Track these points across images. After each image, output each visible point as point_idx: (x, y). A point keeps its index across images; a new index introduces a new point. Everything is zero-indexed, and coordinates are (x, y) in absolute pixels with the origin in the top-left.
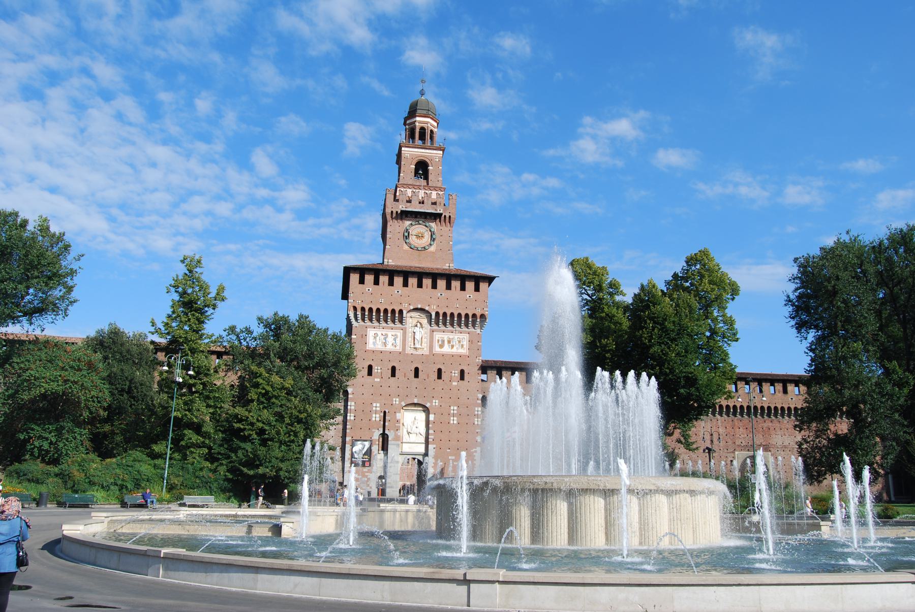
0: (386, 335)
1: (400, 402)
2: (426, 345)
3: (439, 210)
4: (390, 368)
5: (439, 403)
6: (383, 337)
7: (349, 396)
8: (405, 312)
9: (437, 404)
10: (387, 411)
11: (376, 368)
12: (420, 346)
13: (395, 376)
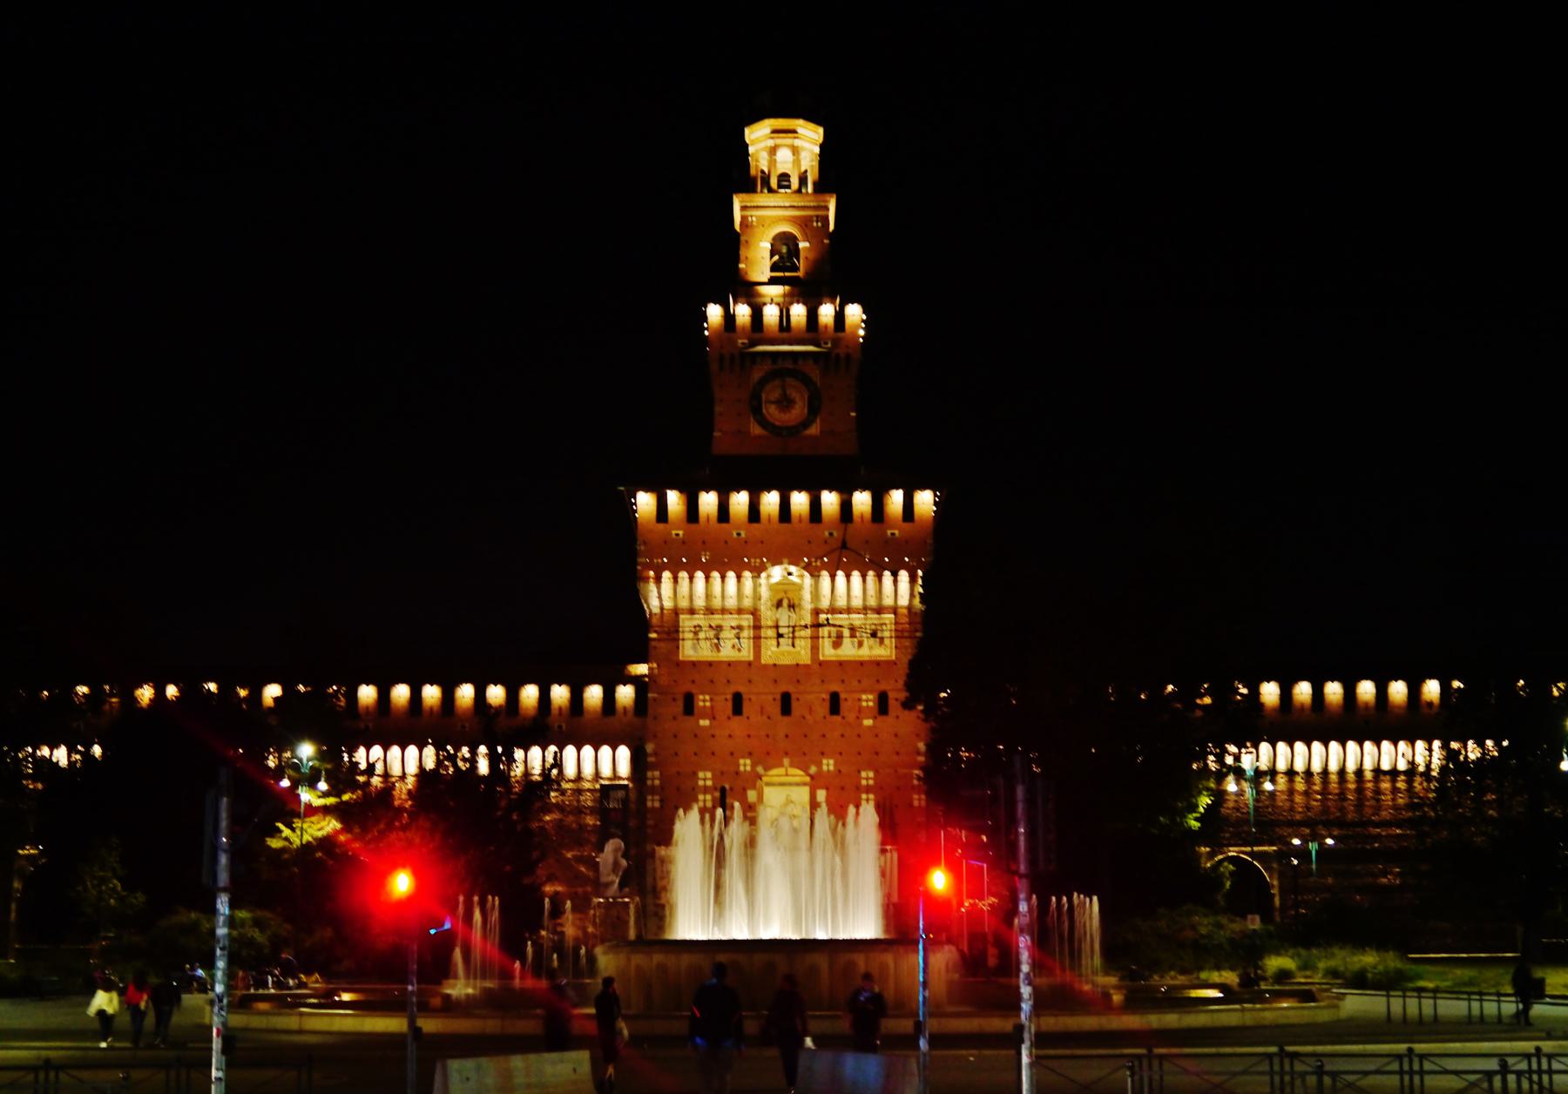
0: (719, 628)
1: (754, 765)
4: (729, 697)
5: (835, 765)
9: (831, 768)
10: (727, 786)
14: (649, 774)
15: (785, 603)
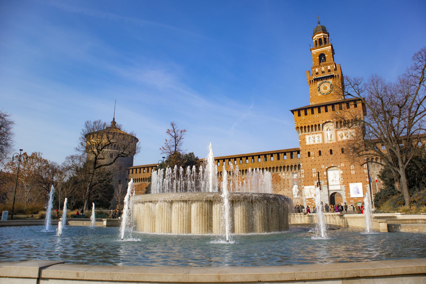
0: (314, 137)
1: (325, 166)
2: (334, 138)
3: (333, 73)
4: (318, 151)
6: (313, 138)
7: (301, 167)
8: (321, 125)
9: (343, 165)
10: (319, 172)
11: (312, 153)
12: (331, 139)
13: (321, 155)
14: (302, 170)
15: (329, 129)
